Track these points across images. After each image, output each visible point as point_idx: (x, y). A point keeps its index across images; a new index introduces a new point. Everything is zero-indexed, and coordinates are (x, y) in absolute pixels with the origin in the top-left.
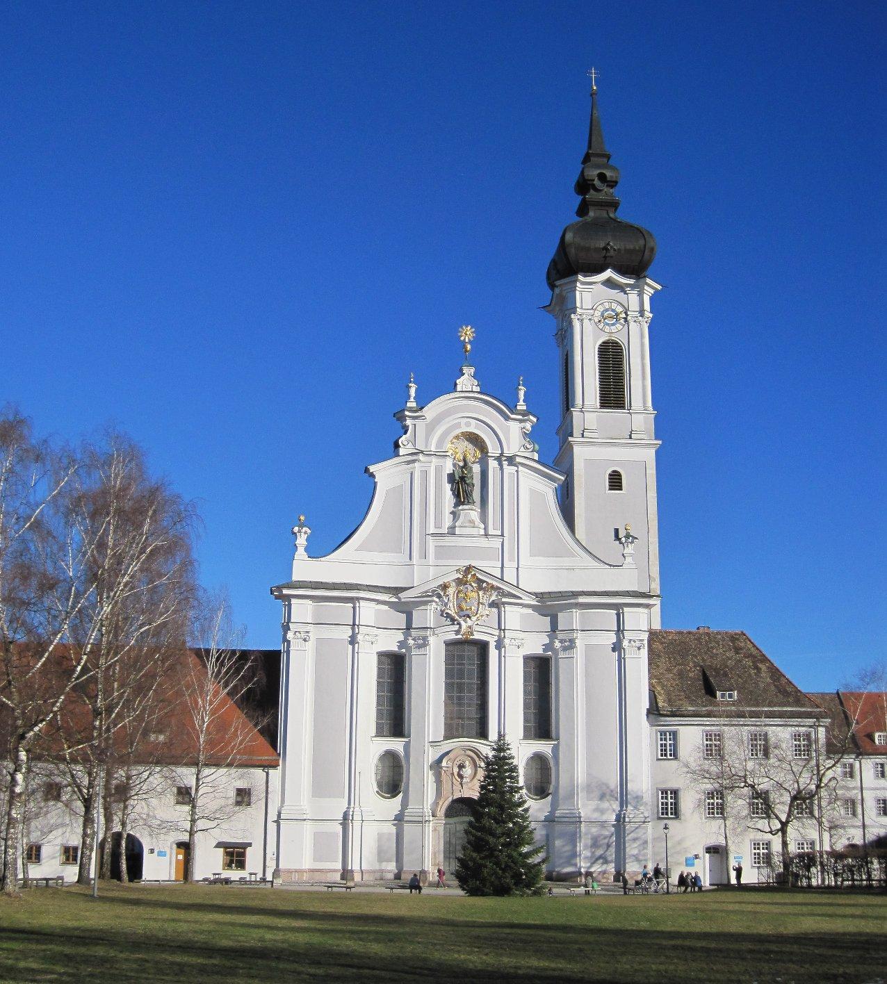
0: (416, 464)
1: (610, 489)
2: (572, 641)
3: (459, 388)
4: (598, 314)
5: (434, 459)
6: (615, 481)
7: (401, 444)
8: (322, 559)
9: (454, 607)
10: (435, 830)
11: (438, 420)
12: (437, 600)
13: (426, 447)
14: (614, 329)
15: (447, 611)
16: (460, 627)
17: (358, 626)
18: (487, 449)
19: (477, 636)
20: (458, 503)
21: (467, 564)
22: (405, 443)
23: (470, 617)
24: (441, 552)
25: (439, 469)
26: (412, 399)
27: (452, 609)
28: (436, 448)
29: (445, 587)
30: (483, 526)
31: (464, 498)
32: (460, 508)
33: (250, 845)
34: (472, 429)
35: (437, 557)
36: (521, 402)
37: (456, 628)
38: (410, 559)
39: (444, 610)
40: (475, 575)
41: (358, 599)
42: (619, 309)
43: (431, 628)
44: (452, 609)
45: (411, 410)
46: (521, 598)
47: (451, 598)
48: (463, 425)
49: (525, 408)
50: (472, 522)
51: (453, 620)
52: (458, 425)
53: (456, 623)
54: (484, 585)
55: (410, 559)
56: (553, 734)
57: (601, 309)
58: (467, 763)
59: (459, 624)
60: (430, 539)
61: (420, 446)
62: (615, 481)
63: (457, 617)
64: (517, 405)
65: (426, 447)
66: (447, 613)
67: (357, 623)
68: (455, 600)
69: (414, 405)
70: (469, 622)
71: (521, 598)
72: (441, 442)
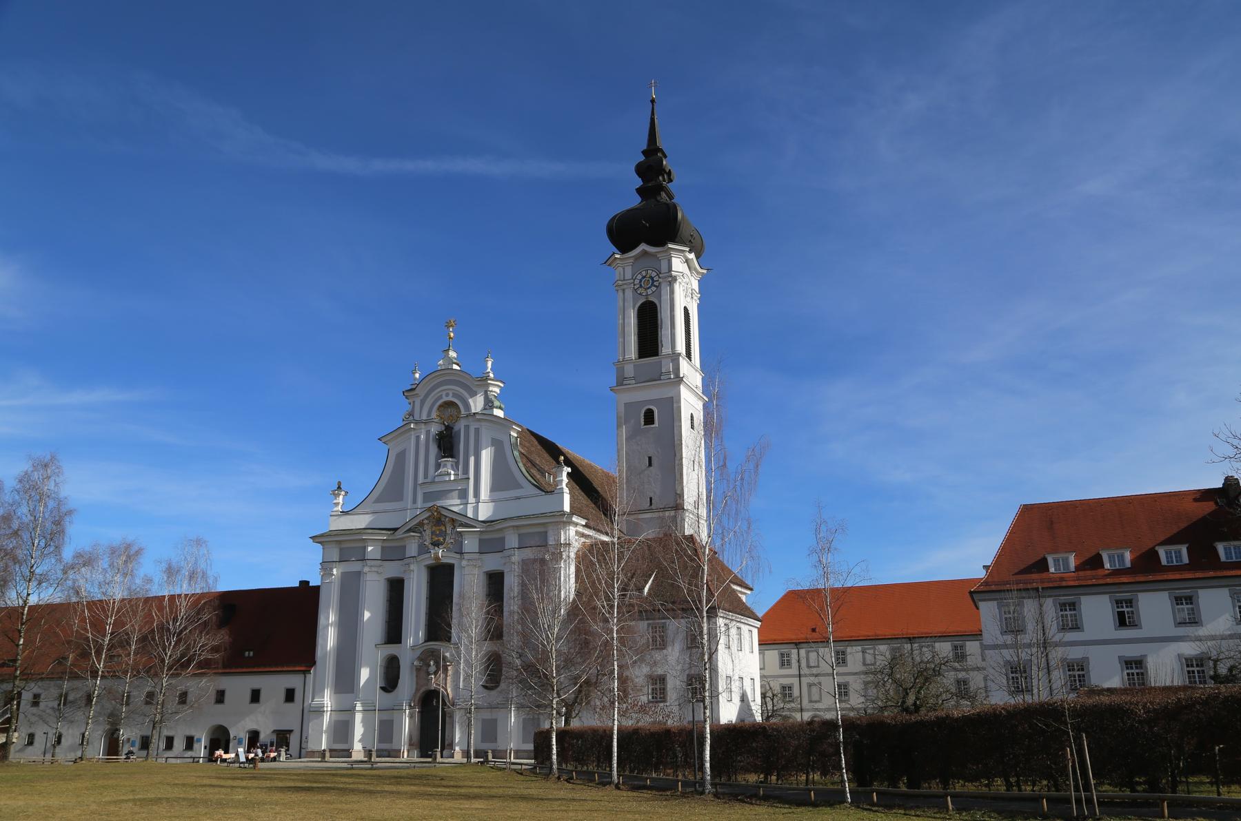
0: (413, 433)
1: (645, 425)
4: (637, 282)
5: (423, 426)
6: (649, 417)
10: (411, 716)
11: (427, 396)
13: (420, 418)
14: (649, 291)
19: (445, 561)
22: (407, 417)
24: (425, 499)
25: (428, 432)
29: (421, 524)
33: (291, 731)
34: (450, 398)
35: (425, 501)
37: (427, 556)
42: (654, 274)
46: (475, 527)
48: (444, 396)
52: (441, 397)
57: (639, 277)
58: (432, 663)
62: (649, 417)
65: (420, 418)
72: (429, 413)
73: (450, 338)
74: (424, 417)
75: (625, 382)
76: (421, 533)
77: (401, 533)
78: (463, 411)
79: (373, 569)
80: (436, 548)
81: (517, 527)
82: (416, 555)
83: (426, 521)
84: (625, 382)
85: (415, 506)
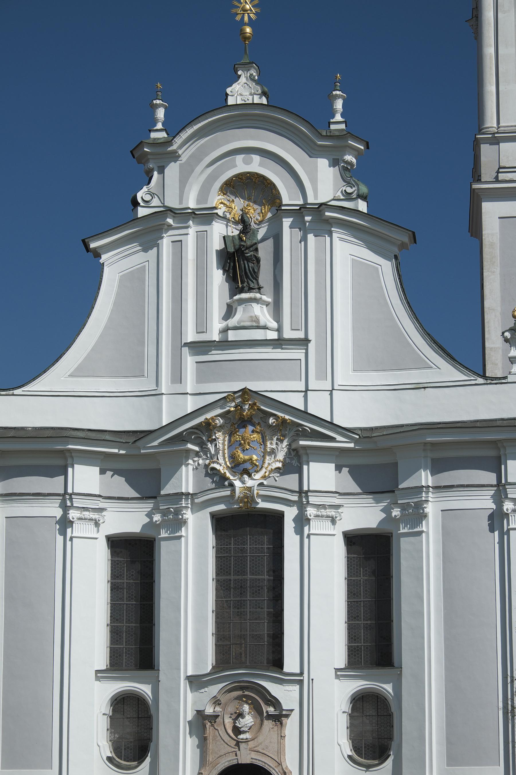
2: (419, 506)
3: (231, 101)
7: (139, 200)
8: (16, 392)
9: (224, 459)
11: (196, 158)
12: (197, 449)
13: (181, 202)
15: (212, 465)
16: (233, 491)
17: (71, 495)
18: (280, 198)
19: (262, 505)
20: (235, 290)
21: (237, 386)
22: (148, 198)
23: (250, 475)
26: (159, 126)
27: (221, 461)
28: (198, 202)
30: (275, 325)
31: (242, 282)
32: (236, 297)
35: (200, 378)
36: (338, 117)
38: (157, 385)
39: (209, 464)
40: (255, 404)
41: (70, 450)
43: (189, 494)
44: (221, 461)
45: (156, 144)
46: (332, 439)
47: (220, 446)
49: (343, 126)
50: (257, 320)
51: (224, 478)
53: (226, 483)
54: (271, 420)
55: (157, 385)
56: (396, 664)
59: (231, 485)
60: (186, 350)
61: (172, 202)
63: (228, 475)
64: (329, 123)
65: (181, 202)
66: (213, 469)
67: (70, 491)
68: (226, 447)
69: (164, 135)
70: (250, 483)
71: (333, 439)
73: (245, 38)
74: (192, 204)
75: (501, 176)
76: (202, 445)
77: (156, 443)
78: (286, 200)
79: (87, 514)
80: (246, 477)
81: (433, 444)
82: (191, 491)
83: (219, 422)
84: (501, 176)
85: (179, 389)
